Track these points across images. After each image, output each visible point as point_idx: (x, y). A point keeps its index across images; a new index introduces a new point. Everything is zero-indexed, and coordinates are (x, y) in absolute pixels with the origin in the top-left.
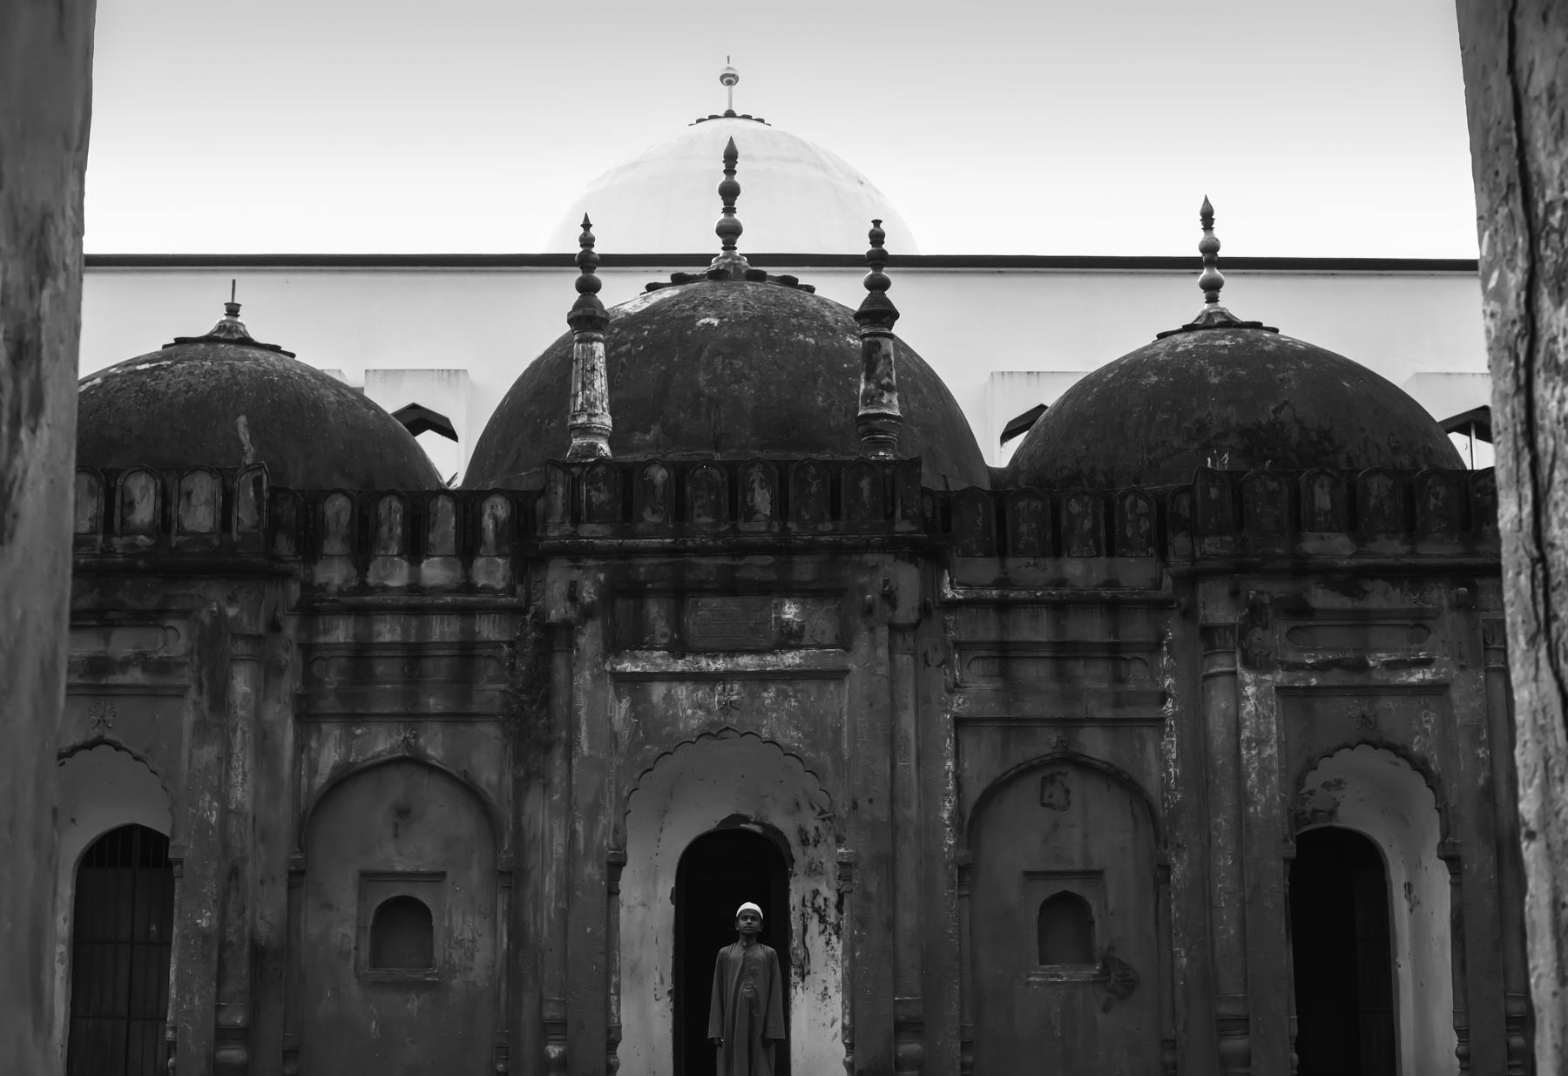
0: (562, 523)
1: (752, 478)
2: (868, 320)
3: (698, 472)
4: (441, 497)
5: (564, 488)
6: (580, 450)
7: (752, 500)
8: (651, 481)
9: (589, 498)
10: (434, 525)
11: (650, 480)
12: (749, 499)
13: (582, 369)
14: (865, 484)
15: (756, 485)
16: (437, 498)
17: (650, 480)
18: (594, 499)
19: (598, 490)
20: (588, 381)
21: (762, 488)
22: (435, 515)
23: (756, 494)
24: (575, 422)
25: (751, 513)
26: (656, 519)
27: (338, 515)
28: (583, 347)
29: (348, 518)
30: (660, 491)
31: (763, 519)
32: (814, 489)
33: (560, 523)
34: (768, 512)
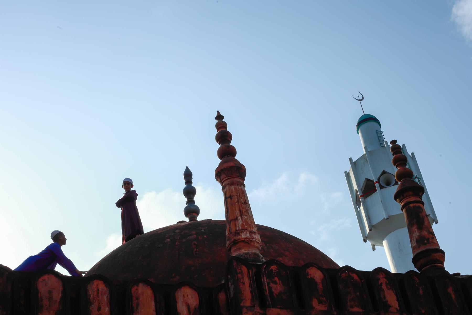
0: (254, 306)
1: (380, 282)
2: (411, 193)
3: (343, 275)
4: (141, 285)
5: (250, 279)
6: (248, 256)
7: (385, 298)
8: (312, 279)
9: (270, 289)
10: (138, 305)
11: (311, 278)
12: (382, 297)
13: (238, 201)
14: (450, 290)
15: (384, 287)
16: (138, 286)
17: (311, 278)
18: (273, 290)
19: (275, 283)
20: (244, 210)
21: (389, 289)
22: (137, 299)
23: (386, 293)
24: (239, 237)
25: (387, 307)
26: (322, 308)
27: (50, 292)
28: (235, 188)
29: (60, 296)
30: (320, 287)
31: (396, 312)
32: (421, 292)
33: (250, 307)
34: (397, 306)
